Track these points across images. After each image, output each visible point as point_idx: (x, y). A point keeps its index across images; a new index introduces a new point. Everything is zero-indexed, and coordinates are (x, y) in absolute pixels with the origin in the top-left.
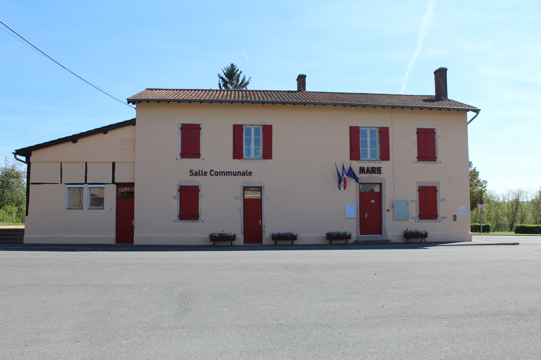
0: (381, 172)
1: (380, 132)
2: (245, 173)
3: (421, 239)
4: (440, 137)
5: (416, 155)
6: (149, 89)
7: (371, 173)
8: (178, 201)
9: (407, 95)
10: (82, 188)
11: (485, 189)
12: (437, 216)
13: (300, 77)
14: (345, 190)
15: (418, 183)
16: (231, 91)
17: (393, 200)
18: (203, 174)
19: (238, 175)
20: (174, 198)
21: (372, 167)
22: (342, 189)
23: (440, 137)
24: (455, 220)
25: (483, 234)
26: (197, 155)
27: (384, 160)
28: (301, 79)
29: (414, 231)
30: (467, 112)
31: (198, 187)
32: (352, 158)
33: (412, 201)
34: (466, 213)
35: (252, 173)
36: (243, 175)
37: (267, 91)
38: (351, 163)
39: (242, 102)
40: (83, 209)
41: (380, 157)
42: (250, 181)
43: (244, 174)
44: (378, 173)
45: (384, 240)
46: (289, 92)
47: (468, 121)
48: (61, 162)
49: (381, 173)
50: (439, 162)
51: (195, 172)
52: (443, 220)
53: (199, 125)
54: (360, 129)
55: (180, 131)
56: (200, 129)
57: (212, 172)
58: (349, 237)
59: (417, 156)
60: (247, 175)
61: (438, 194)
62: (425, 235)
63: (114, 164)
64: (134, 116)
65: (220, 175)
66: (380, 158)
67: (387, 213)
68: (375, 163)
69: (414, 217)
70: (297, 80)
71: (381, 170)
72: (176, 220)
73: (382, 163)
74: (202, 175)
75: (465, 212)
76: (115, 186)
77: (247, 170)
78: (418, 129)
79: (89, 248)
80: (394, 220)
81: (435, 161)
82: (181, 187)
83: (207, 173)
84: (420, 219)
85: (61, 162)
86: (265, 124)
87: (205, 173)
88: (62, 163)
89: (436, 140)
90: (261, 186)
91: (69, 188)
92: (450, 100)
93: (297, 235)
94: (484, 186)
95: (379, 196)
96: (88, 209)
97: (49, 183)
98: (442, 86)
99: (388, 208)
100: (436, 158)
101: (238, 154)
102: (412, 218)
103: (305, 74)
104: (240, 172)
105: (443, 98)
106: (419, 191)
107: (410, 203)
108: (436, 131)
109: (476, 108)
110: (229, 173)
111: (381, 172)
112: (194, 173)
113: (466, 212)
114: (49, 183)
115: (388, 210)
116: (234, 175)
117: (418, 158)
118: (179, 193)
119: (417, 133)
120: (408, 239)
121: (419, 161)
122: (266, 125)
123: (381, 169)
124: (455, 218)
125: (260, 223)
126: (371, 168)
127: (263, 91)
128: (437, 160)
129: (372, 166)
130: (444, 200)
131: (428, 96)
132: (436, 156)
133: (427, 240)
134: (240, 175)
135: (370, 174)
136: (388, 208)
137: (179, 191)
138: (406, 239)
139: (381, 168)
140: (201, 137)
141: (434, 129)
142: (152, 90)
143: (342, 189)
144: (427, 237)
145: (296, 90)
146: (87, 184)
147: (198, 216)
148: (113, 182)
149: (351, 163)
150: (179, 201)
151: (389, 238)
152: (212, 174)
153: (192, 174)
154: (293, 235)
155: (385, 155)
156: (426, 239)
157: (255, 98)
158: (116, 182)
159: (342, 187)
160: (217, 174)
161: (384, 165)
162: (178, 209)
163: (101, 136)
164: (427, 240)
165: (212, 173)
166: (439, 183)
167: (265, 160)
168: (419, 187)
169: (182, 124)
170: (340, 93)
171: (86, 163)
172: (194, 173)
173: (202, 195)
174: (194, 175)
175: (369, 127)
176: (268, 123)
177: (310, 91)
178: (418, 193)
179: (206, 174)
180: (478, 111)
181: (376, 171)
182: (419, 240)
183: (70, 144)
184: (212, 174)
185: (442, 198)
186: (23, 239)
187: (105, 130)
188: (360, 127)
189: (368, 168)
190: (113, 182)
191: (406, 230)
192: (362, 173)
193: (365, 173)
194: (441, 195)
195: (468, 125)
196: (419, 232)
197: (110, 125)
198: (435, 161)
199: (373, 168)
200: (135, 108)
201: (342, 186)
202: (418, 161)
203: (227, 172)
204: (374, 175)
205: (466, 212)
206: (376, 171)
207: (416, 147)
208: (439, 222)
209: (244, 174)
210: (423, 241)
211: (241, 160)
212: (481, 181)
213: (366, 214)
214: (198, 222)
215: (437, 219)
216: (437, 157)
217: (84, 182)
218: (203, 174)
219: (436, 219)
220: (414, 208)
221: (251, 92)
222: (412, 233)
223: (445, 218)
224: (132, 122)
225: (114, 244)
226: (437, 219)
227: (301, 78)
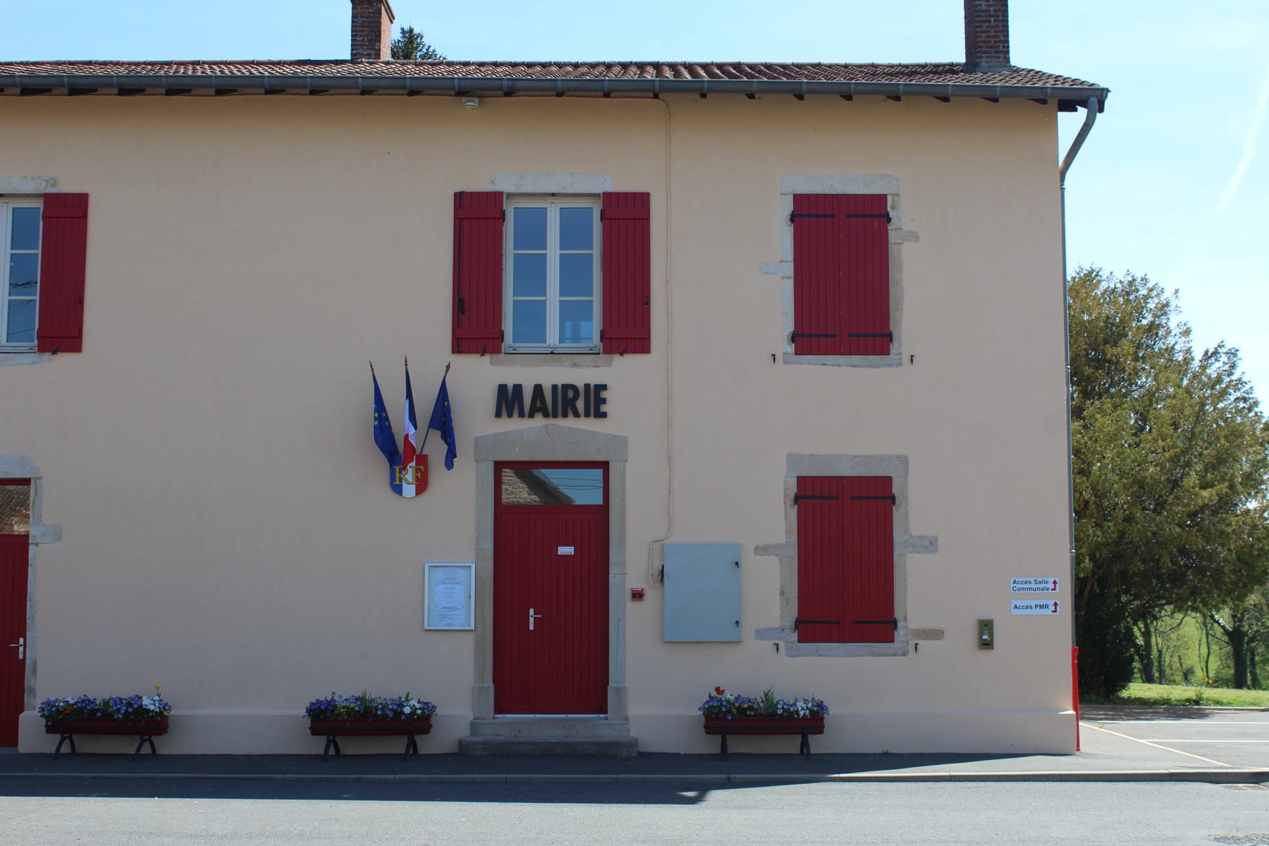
0: (604, 408)
4: (915, 237)
5: (787, 324)
7: (555, 416)
12: (894, 624)
14: (425, 496)
15: (793, 459)
17: (663, 545)
21: (560, 382)
22: (409, 490)
23: (915, 237)
24: (987, 645)
32: (461, 344)
33: (762, 550)
34: (1049, 611)
38: (448, 367)
44: (587, 415)
49: (604, 415)
50: (906, 359)
52: (923, 644)
59: (790, 327)
61: (897, 514)
62: (815, 721)
66: (601, 340)
67: (633, 607)
68: (574, 365)
69: (773, 629)
71: (604, 401)
73: (609, 364)
75: (1042, 607)
78: (799, 199)
81: (885, 351)
84: (802, 639)
86: (55, 190)
89: (893, 249)
90: (27, 476)
93: (165, 707)
99: (635, 583)
100: (890, 337)
102: (761, 634)
106: (797, 499)
107: (751, 561)
108: (892, 207)
111: (604, 408)
113: (1047, 606)
115: (638, 595)
117: (794, 338)
119: (793, 218)
122: (58, 195)
123: (604, 394)
124: (985, 635)
125: (21, 649)
126: (555, 387)
128: (894, 348)
129: (560, 381)
130: (931, 545)
132: (892, 328)
135: (551, 421)
136: (637, 586)
141: (882, 198)
143: (409, 490)
144: (819, 729)
149: (448, 367)
151: (633, 733)
154: (142, 710)
159: (408, 483)
166: (903, 460)
167: (47, 356)
168: (802, 480)
175: (553, 195)
176: (67, 186)
178: (794, 512)
181: (580, 405)
185: (923, 537)
188: (510, 195)
189: (538, 389)
191: (714, 694)
192: (510, 415)
193: (521, 415)
196: (775, 706)
198: (885, 351)
199: (566, 387)
201: (410, 475)
202: (797, 353)
204: (571, 423)
205: (1047, 606)
206: (580, 405)
207: (790, 284)
208: (904, 654)
213: (532, 611)
215: (893, 642)
216: (895, 335)
219: (890, 639)
223: (936, 634)
226: (893, 642)
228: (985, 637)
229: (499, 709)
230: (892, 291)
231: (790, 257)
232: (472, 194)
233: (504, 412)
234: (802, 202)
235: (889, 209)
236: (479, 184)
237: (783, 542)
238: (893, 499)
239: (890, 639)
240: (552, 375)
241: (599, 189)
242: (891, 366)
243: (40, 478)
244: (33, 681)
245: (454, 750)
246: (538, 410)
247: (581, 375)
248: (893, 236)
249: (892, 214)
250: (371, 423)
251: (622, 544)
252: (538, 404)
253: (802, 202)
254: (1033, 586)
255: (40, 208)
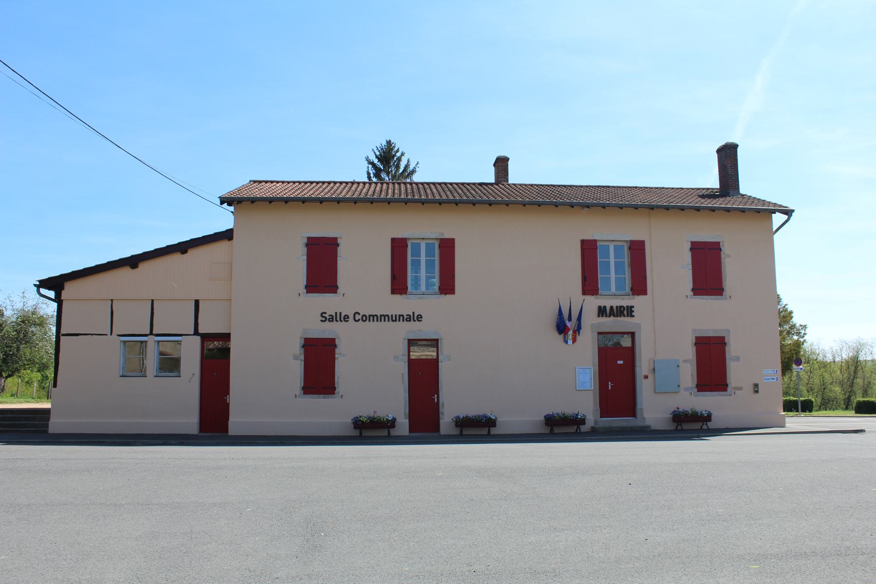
0: (633, 314)
1: (630, 248)
2: (410, 318)
3: (701, 424)
4: (729, 256)
5: (690, 285)
6: (255, 182)
7: (617, 316)
8: (301, 364)
9: (673, 189)
10: (146, 342)
11: (804, 338)
12: (727, 385)
13: (499, 160)
14: (575, 344)
15: (694, 331)
16: (388, 184)
17: (654, 361)
18: (342, 319)
19: (399, 321)
20: (295, 358)
21: (618, 305)
22: (570, 342)
23: (729, 256)
24: (757, 392)
25: (802, 415)
26: (332, 288)
27: (638, 295)
28: (501, 164)
29: (690, 411)
30: (773, 215)
31: (334, 340)
32: (584, 293)
33: (684, 361)
34: (775, 380)
35: (421, 317)
36: (407, 321)
37: (445, 184)
38: (584, 300)
39: (406, 202)
40: (146, 377)
41: (632, 289)
42: (420, 330)
43: (409, 319)
44: (628, 316)
45: (639, 427)
46: (481, 184)
47: (774, 229)
48: (112, 300)
49: (633, 316)
50: (728, 297)
51: (330, 316)
52: (737, 392)
53: (335, 239)
54: (598, 244)
55: (305, 249)
56: (338, 245)
57: (357, 315)
58: (582, 421)
59: (691, 286)
60: (414, 321)
61: (727, 349)
62: (708, 418)
63: (197, 302)
64: (230, 226)
65: (369, 321)
67: (645, 381)
68: (623, 299)
69: (690, 388)
70: (495, 165)
71: (633, 311)
72: (298, 394)
73: (634, 299)
74: (341, 321)
75: (773, 379)
76: (198, 338)
77: (414, 313)
78: (693, 243)
79: (154, 441)
80: (655, 393)
81: (721, 295)
82: (306, 340)
83: (348, 318)
84: (698, 391)
85: (112, 300)
86: (442, 237)
87: (346, 318)
88: (114, 301)
89: (723, 260)
90: (437, 338)
91: (125, 342)
92: (743, 195)
93: (496, 418)
94: (802, 334)
95: (630, 354)
96: (155, 376)
97: (92, 334)
98: (731, 173)
99: (645, 373)
100: (723, 290)
101: (399, 285)
102: (686, 389)
103: (507, 156)
104: (403, 316)
105: (732, 193)
106: (696, 344)
107: (682, 365)
109: (786, 207)
110: (384, 317)
111: (633, 314)
112: (328, 317)
114: (92, 334)
115: (646, 377)
116: (393, 321)
117: (693, 290)
118: (303, 349)
119: (691, 249)
120: (679, 423)
121: (694, 295)
123: (633, 309)
124: (756, 388)
126: (617, 307)
127: (440, 184)
128: (724, 293)
129: (618, 305)
131: (708, 189)
132: (723, 287)
133: (711, 425)
134: (403, 321)
136: (646, 374)
137: (303, 346)
138: (676, 424)
139: (633, 307)
140: (338, 258)
141: (718, 243)
142: (260, 182)
143: (570, 342)
145: (493, 181)
146: (154, 335)
147: (335, 388)
148: (196, 333)
149: (584, 300)
150: (303, 363)
151: (648, 423)
152: (357, 319)
153: (324, 319)
154: (490, 418)
155: (639, 287)
156: (708, 423)
157: (427, 195)
158: (201, 331)
160: (365, 318)
161: (638, 302)
162: (301, 377)
163: (177, 257)
164: (711, 425)
165: (358, 317)
166: (728, 331)
167: (443, 295)
168: (697, 338)
169: (309, 238)
170: (565, 186)
171: (153, 301)
172: (328, 317)
173: (340, 354)
174: (327, 321)
175: (613, 241)
176: (447, 236)
177: (515, 183)
179: (346, 318)
180: (790, 213)
181: (625, 312)
182: (697, 426)
183: (126, 271)
184: (357, 319)
186: (47, 426)
187: (183, 248)
188: (599, 240)
189: (612, 307)
190: (196, 333)
191: (676, 409)
192: (603, 316)
193: (606, 316)
194: (732, 350)
195: (776, 236)
196: (698, 413)
197: (192, 240)
198: (721, 295)
199: (621, 307)
200: (232, 212)
201: (570, 337)
203: (381, 316)
204: (622, 319)
206: (625, 312)
207: (690, 272)
208: (731, 395)
209: (409, 319)
210: (705, 427)
211: (404, 296)
212: (798, 325)
213: (610, 383)
214: (335, 398)
217: (148, 333)
218: (342, 319)
219: (726, 390)
220: (688, 374)
221: (420, 186)
222: (686, 415)
223: (740, 389)
224: (227, 235)
225: (196, 434)
227: (501, 162)
228: (756, 389)
229: (601, 417)
230: (723, 275)
231: (691, 263)
232: (587, 240)
233: (601, 316)
234: (694, 244)
235: (721, 247)
236: (588, 237)
237: (691, 358)
238: (725, 344)
239: (726, 390)
240: (616, 302)
241: (628, 239)
242: (723, 299)
243: (442, 339)
244: (443, 410)
245: (590, 430)
246: (612, 315)
247: (625, 302)
248: (723, 256)
249: (722, 248)
250: (556, 320)
251: (640, 360)
252: (612, 313)
253: (694, 244)
254: (770, 372)
255: (426, 243)
